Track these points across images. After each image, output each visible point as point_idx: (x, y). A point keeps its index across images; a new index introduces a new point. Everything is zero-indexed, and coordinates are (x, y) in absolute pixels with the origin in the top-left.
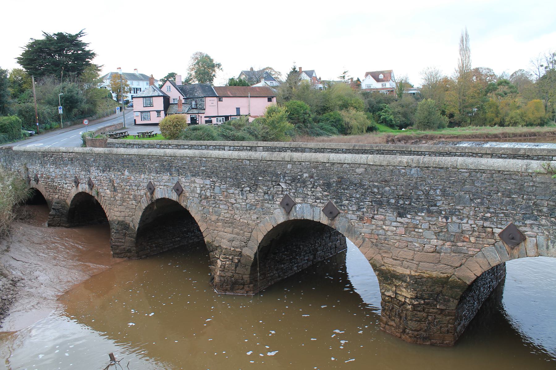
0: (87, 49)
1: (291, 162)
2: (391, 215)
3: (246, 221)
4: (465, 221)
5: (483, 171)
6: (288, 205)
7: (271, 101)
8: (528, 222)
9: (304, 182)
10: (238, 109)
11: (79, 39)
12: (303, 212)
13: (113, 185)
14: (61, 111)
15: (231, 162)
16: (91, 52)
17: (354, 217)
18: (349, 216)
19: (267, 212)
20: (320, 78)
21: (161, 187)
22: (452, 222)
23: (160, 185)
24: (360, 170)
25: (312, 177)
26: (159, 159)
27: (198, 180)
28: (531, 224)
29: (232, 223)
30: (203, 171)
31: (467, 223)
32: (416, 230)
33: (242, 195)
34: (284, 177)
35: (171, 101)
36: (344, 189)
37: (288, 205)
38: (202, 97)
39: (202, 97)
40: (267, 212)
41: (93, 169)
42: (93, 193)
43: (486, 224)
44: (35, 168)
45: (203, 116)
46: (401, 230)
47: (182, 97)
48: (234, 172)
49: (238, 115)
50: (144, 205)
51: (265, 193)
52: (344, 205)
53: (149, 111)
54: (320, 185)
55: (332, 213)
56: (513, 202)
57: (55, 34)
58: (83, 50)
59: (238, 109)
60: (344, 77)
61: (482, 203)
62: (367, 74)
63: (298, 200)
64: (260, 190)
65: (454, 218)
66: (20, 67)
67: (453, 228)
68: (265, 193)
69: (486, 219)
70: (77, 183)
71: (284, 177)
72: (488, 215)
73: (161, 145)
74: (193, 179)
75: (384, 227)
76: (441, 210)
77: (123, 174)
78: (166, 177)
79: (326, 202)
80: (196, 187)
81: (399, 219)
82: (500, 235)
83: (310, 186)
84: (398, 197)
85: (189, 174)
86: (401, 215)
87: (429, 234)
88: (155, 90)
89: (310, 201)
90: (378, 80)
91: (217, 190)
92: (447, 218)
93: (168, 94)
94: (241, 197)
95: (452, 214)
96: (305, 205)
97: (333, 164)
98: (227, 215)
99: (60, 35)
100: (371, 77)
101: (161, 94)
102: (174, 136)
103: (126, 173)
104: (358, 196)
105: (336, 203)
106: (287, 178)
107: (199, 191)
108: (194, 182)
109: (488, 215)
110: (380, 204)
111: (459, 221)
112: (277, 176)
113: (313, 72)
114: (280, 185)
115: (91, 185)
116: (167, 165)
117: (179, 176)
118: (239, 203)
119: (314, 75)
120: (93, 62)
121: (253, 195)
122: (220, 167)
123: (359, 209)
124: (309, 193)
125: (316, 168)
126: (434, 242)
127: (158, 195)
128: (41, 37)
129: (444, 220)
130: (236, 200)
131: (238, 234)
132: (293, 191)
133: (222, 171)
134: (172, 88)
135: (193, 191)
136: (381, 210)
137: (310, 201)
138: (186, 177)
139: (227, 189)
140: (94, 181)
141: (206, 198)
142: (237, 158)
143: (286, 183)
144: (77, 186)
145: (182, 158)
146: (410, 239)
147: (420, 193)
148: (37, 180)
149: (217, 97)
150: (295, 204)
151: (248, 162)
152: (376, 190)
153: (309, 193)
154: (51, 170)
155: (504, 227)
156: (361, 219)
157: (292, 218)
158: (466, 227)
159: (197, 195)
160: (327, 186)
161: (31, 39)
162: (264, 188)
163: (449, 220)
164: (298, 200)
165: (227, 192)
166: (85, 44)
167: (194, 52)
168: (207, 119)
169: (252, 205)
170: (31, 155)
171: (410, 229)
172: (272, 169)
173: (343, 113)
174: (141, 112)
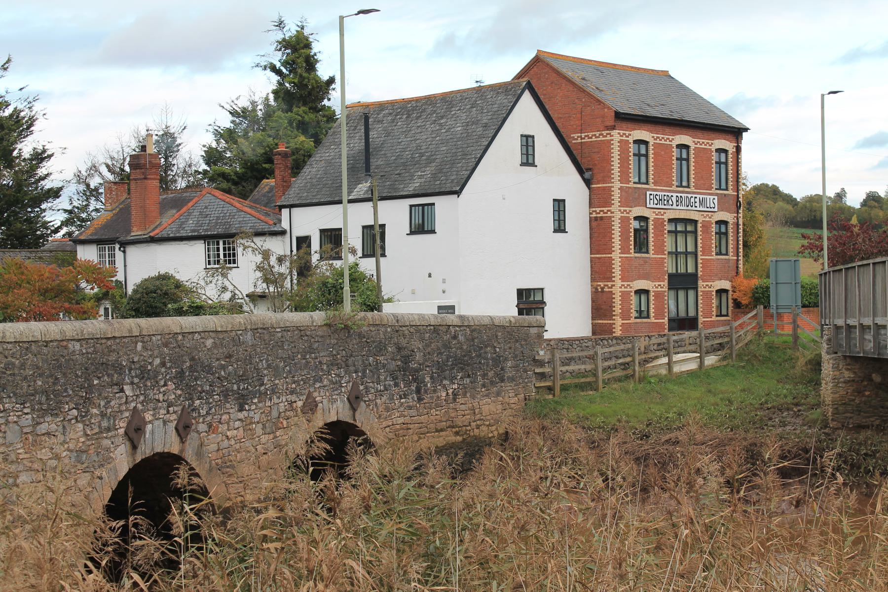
8: (318, 385)
15: (45, 350)
25: (163, 364)
48: (51, 376)
54: (171, 379)
61: (290, 372)
63: (148, 416)
64: (95, 411)
67: (275, 414)
69: (292, 393)
79: (178, 409)
81: (241, 415)
86: (241, 409)
94: (61, 438)
112: (119, 369)
121: (80, 425)
122: (23, 366)
125: (166, 345)
132: (142, 398)
133: (25, 378)
142: (58, 337)
143: (132, 383)
151: (77, 346)
171: (247, 424)
172: (113, 357)
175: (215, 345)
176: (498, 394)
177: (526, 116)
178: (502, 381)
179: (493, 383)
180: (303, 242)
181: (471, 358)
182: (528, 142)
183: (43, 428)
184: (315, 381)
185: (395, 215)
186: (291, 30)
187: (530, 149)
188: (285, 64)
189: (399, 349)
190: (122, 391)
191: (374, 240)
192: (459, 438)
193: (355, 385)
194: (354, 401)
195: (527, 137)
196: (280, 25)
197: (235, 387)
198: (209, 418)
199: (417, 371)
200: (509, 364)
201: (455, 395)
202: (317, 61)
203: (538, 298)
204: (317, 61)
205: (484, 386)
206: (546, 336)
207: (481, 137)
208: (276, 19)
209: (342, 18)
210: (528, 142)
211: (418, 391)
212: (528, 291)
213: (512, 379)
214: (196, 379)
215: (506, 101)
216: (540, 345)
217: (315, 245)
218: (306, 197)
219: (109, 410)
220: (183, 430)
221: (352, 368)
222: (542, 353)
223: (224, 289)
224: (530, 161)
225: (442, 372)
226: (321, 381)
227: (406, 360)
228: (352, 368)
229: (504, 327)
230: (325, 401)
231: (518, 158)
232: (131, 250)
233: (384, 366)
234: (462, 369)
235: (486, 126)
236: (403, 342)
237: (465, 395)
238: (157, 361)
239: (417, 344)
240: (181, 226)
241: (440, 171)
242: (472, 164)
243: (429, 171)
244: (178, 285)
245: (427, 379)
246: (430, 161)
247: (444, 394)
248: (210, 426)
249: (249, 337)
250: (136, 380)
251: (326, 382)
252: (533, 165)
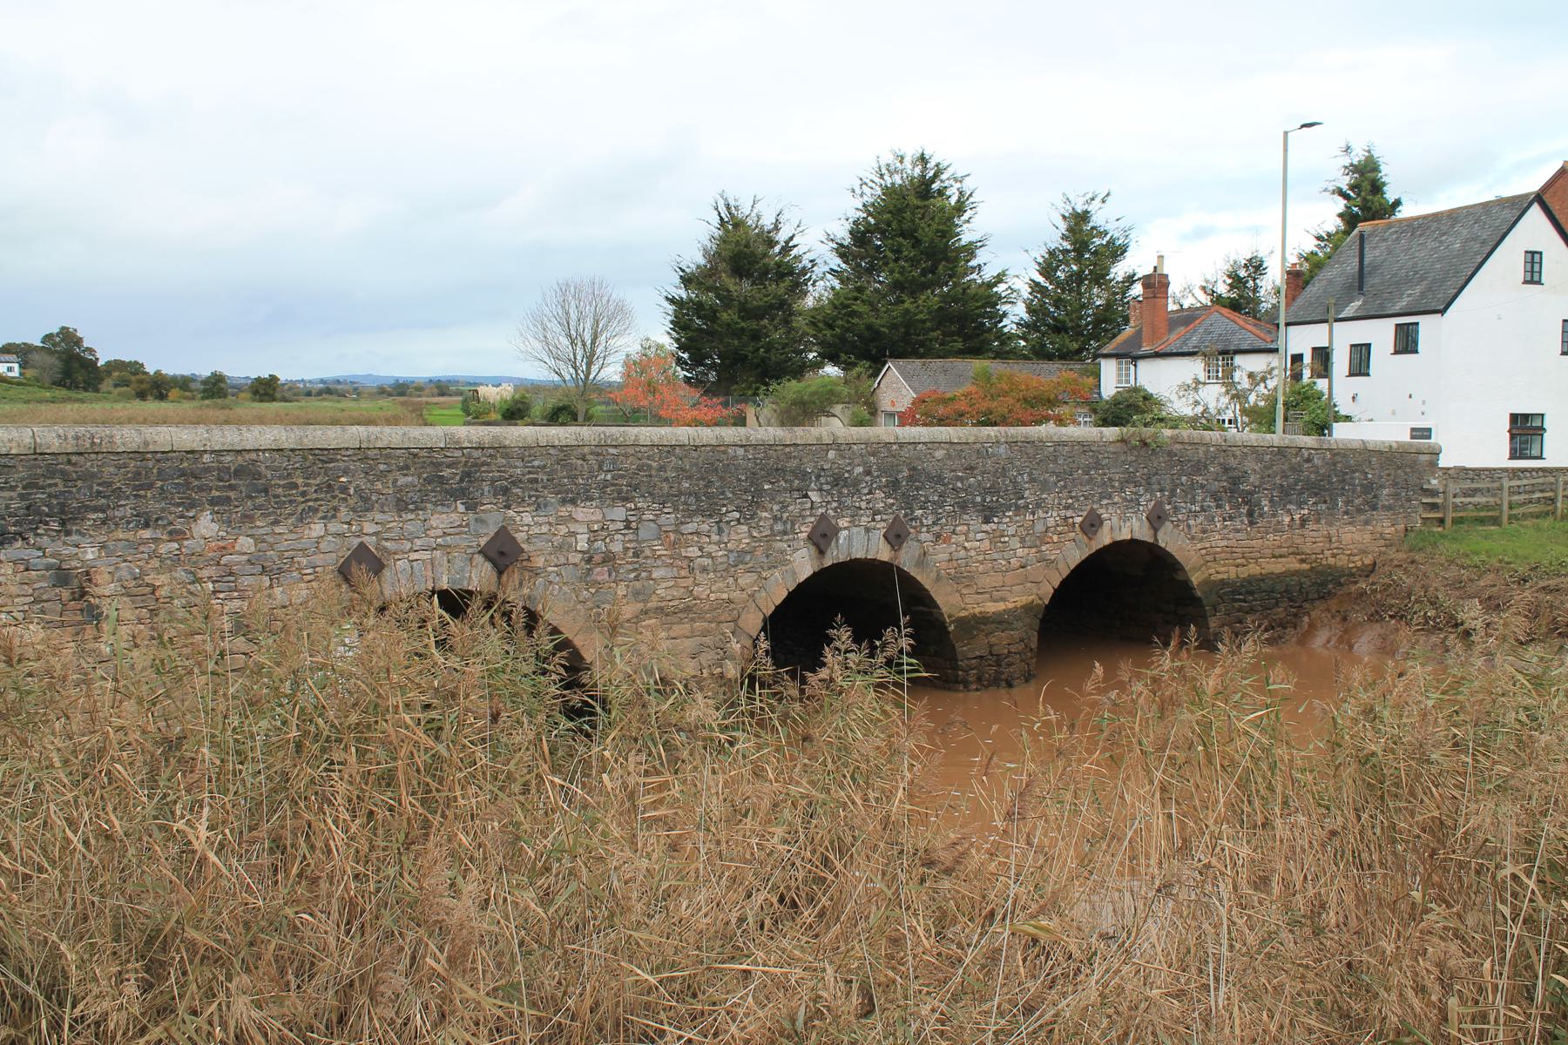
2: (975, 522)
3: (725, 596)
6: (822, 537)
8: (1105, 502)
9: (856, 483)
12: (850, 546)
15: (694, 454)
17: (929, 537)
18: (923, 537)
19: (779, 561)
21: (414, 556)
23: (411, 550)
24: (939, 454)
25: (868, 473)
26: (413, 458)
30: (605, 484)
33: (720, 532)
34: (818, 477)
37: (822, 537)
40: (779, 561)
43: (1069, 513)
46: (987, 543)
48: (703, 479)
51: (776, 519)
52: (914, 519)
54: (879, 488)
56: (1091, 479)
61: (1065, 487)
63: (843, 523)
67: (1039, 527)
68: (776, 519)
69: (1067, 507)
71: (818, 477)
74: (564, 511)
79: (890, 518)
80: (574, 534)
81: (986, 527)
84: (987, 491)
85: (552, 498)
86: (987, 521)
91: (647, 531)
94: (715, 538)
95: (1038, 506)
96: (855, 530)
97: (901, 445)
103: (206, 526)
105: (906, 515)
106: (823, 480)
107: (582, 545)
108: (571, 518)
112: (804, 476)
117: (508, 507)
118: (709, 555)
121: (745, 528)
122: (662, 468)
124: (863, 505)
126: (1020, 552)
130: (701, 549)
132: (834, 505)
133: (666, 480)
141: (609, 558)
142: (714, 442)
143: (820, 490)
146: (996, 556)
150: (837, 530)
151: (741, 452)
157: (828, 563)
159: (576, 558)
160: (894, 485)
162: (776, 507)
164: (843, 523)
165: (676, 531)
169: (744, 552)
171: (996, 537)
175: (949, 456)
176: (1366, 523)
177: (1535, 229)
178: (1374, 508)
179: (1359, 511)
180: (1297, 358)
181: (1330, 483)
182: (1533, 260)
183: (691, 527)
185: (1380, 334)
186: (1358, 156)
187: (1536, 268)
188: (1352, 187)
189: (1226, 470)
190: (806, 496)
191: (1361, 360)
192: (1305, 566)
193: (1159, 504)
194: (1156, 519)
195: (1533, 253)
196: (1347, 149)
197: (979, 499)
198: (937, 528)
199: (1251, 493)
200: (1386, 492)
201: (1304, 521)
202: (1384, 184)
203: (1537, 423)
204: (1384, 184)
205: (1346, 513)
206: (1442, 464)
207: (1477, 254)
208: (1343, 145)
209: (1286, 133)
210: (1533, 260)
211: (1250, 514)
212: (1526, 417)
213: (1389, 508)
214: (917, 489)
215: (1509, 215)
216: (1433, 473)
217: (1307, 359)
218: (1302, 316)
219: (785, 515)
220: (896, 537)
221: (1156, 487)
222: (1434, 482)
223: (1197, 403)
224: (1536, 278)
225: (1285, 496)
227: (1235, 481)
228: (1156, 487)
229: (1380, 452)
230: (1115, 519)
231: (1520, 275)
232: (1141, 364)
233: (1202, 486)
234: (1316, 494)
235: (1484, 242)
236: (1233, 462)
237: (1318, 521)
239: (1250, 465)
240: (1185, 343)
241: (1429, 289)
242: (1461, 282)
243: (1418, 290)
244: (1147, 398)
245: (1265, 502)
246: (1422, 279)
247: (1287, 519)
248: (938, 536)
249: (1002, 449)
251: (1116, 499)
252: (1539, 283)
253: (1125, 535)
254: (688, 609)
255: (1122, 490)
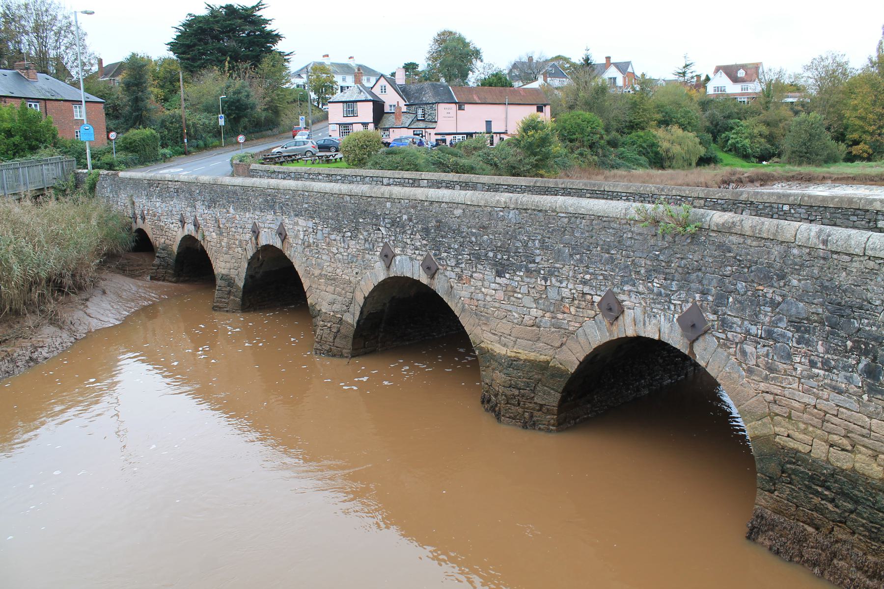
0: (269, 28)
1: (390, 199)
2: (490, 274)
4: (564, 285)
5: (583, 216)
6: (388, 258)
7: (542, 111)
9: (403, 226)
10: (489, 123)
11: (258, 13)
12: (402, 267)
13: (219, 227)
14: (222, 122)
15: (332, 198)
16: (274, 33)
17: (453, 275)
18: (448, 273)
19: (367, 266)
20: (643, 75)
22: (552, 285)
24: (458, 212)
25: (410, 220)
27: (301, 221)
28: (630, 291)
29: (334, 279)
30: (306, 210)
31: (567, 287)
32: (516, 295)
35: (387, 109)
36: (442, 237)
37: (388, 258)
38: (433, 104)
39: (433, 104)
40: (367, 266)
41: (198, 204)
42: (199, 238)
43: (586, 289)
44: (142, 202)
45: (433, 132)
46: (500, 295)
47: (402, 103)
49: (489, 132)
50: (250, 254)
53: (352, 124)
55: (431, 270)
56: (612, 260)
57: (222, 7)
58: (262, 31)
59: (489, 123)
60: (684, 73)
61: (581, 261)
62: (718, 69)
63: (397, 251)
64: (361, 237)
65: (554, 280)
66: (172, 55)
68: (366, 240)
69: (585, 283)
70: (183, 222)
72: (588, 277)
73: (309, 174)
75: (483, 290)
76: (540, 269)
77: (228, 212)
78: (270, 216)
80: (299, 231)
82: (599, 304)
83: (409, 232)
84: (497, 250)
86: (499, 274)
87: (528, 301)
88: (361, 91)
89: (409, 252)
90: (735, 80)
92: (546, 281)
93: (383, 97)
95: (551, 274)
96: (404, 257)
97: (432, 202)
98: (330, 269)
99: (230, 8)
100: (724, 75)
101: (370, 98)
102: (360, 163)
103: (231, 210)
104: (456, 247)
105: (435, 255)
106: (387, 221)
107: (302, 237)
108: (297, 224)
109: (588, 277)
110: (477, 258)
111: (558, 284)
112: (377, 217)
113: (628, 64)
114: (379, 230)
115: (196, 225)
116: (271, 201)
119: (630, 70)
120: (279, 47)
123: (457, 264)
124: (409, 241)
125: (415, 207)
126: (534, 312)
127: (263, 241)
128: (203, 12)
129: (543, 282)
131: (340, 295)
132: (393, 238)
134: (389, 88)
135: (296, 236)
136: (479, 266)
137: (409, 252)
138: (290, 217)
139: (329, 234)
140: (200, 221)
144: (183, 227)
145: (286, 191)
146: (509, 307)
147: (519, 244)
148: (143, 218)
149: (456, 103)
152: (473, 239)
153: (409, 241)
154: (158, 204)
155: (603, 294)
156: (460, 277)
158: (566, 293)
161: (190, 15)
163: (548, 283)
166: (266, 22)
167: (441, 29)
168: (439, 137)
170: (136, 183)
172: (371, 208)
173: (660, 133)
174: (340, 124)
183: (333, 237)
184: (623, 283)
197: (491, 254)
221: (695, 286)
226: (634, 285)
230: (639, 311)
233: (774, 305)
238: (405, 217)
250: (388, 226)
253: (650, 332)
254: (334, 279)
255: (648, 279)
